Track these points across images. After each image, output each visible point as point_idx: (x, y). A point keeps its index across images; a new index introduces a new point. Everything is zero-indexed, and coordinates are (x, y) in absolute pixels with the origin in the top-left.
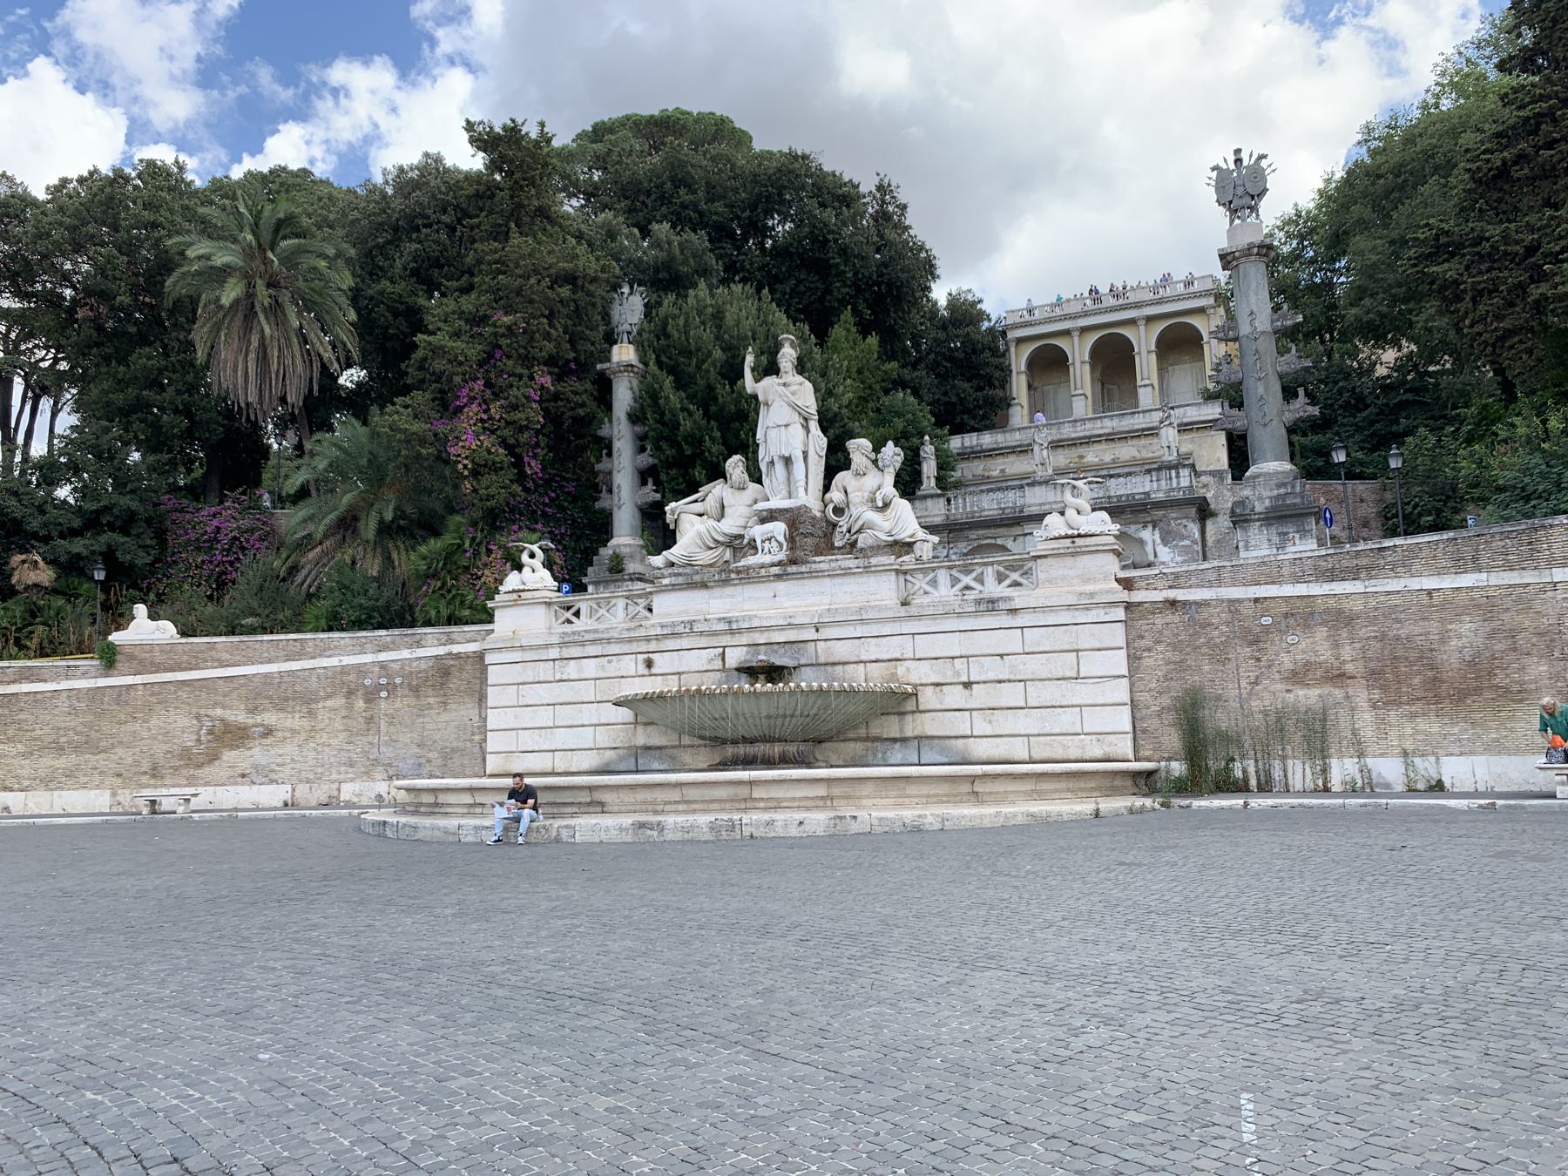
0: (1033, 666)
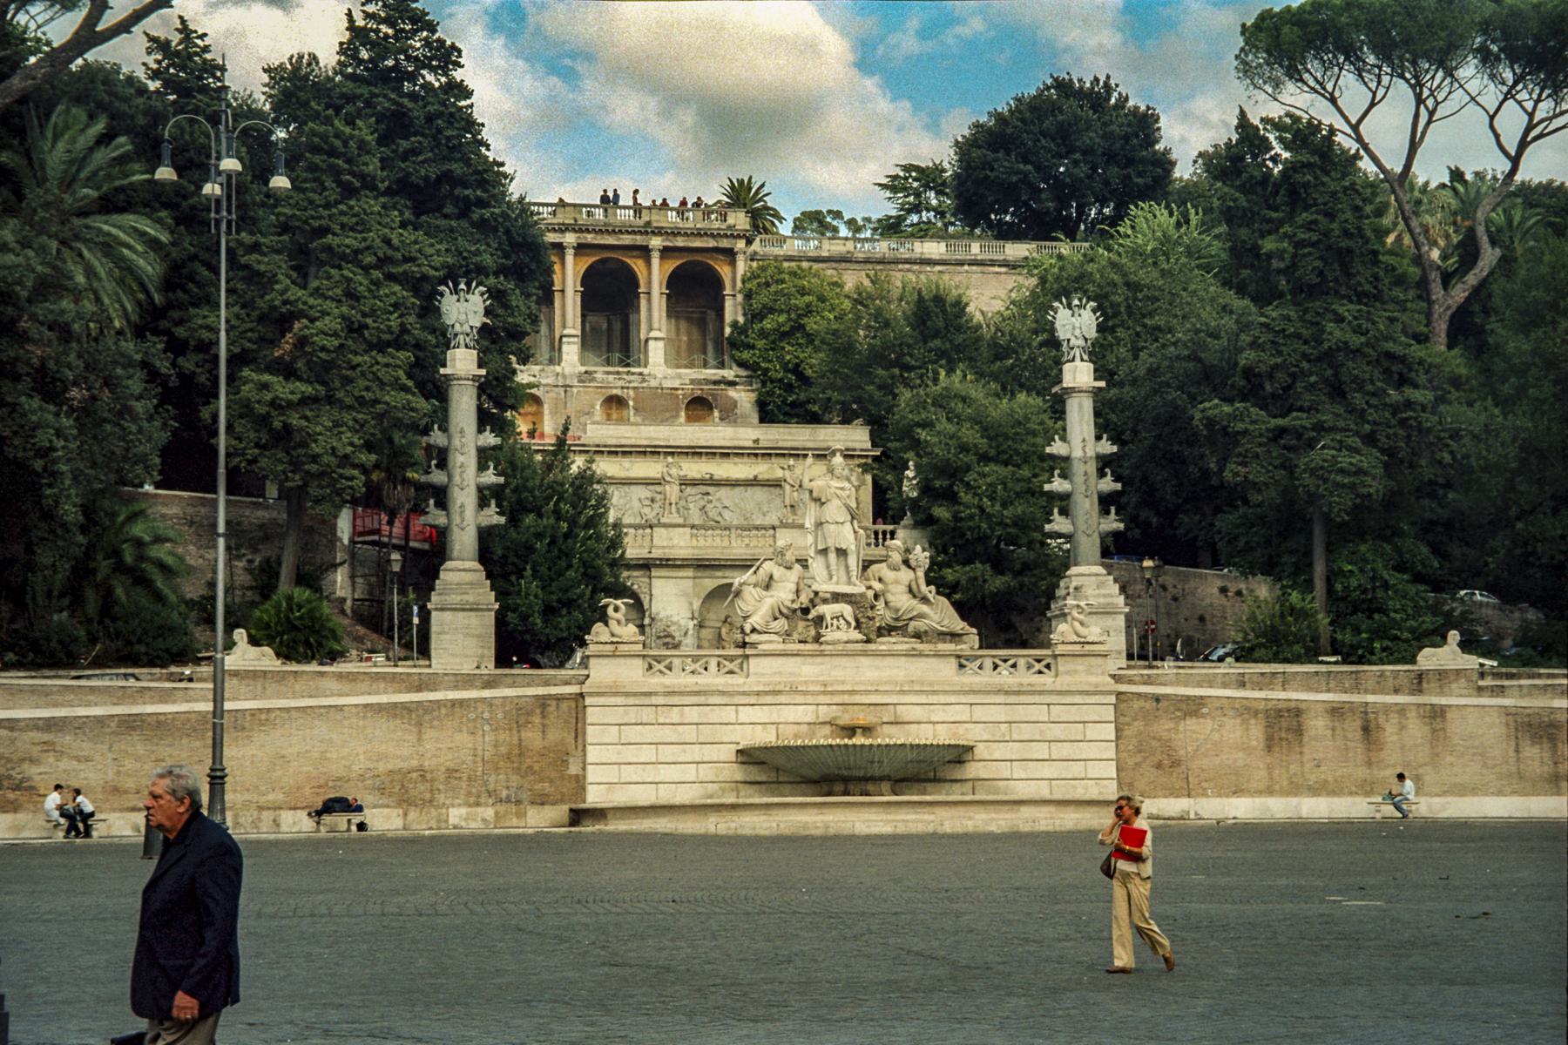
0: (1056, 731)
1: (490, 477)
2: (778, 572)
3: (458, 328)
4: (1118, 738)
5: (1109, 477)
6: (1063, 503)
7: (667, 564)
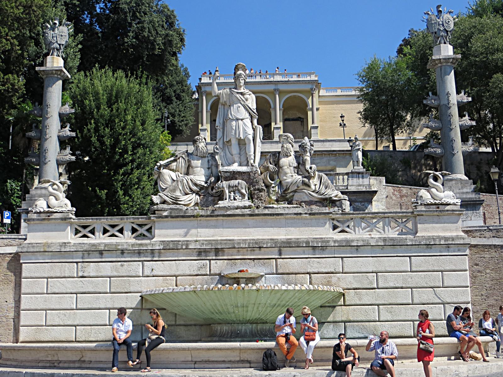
1: (67, 132)
4: (473, 283)
5: (467, 117)
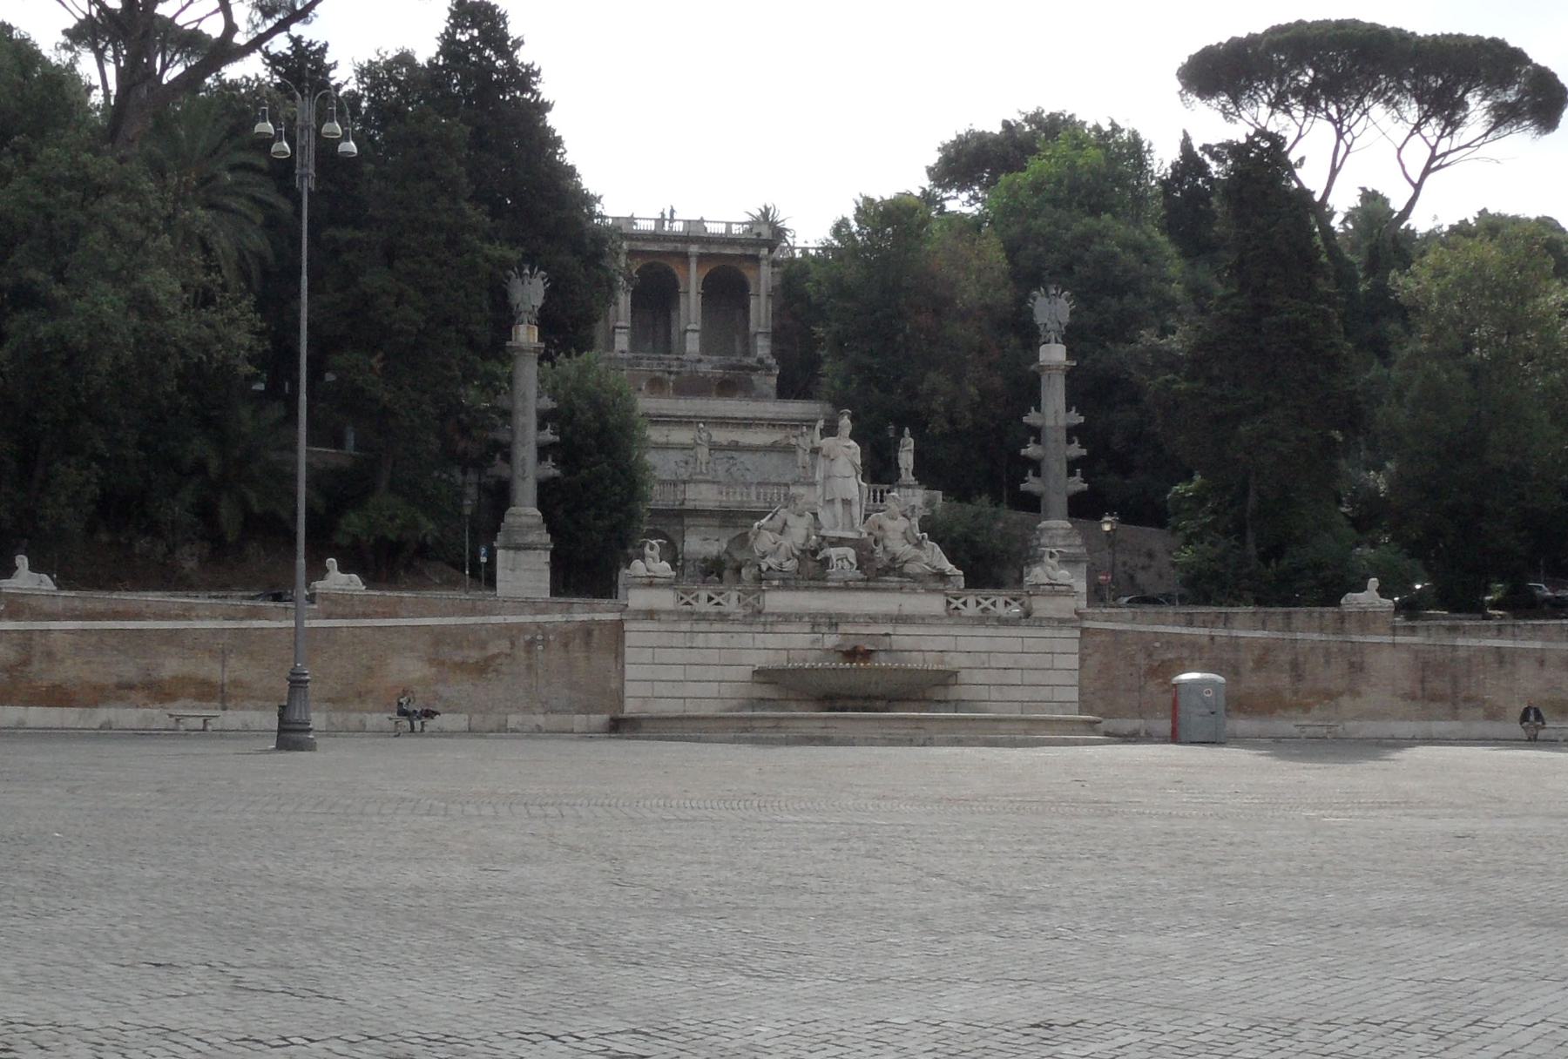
0: (1028, 660)
1: (548, 436)
2: (792, 519)
3: (522, 307)
6: (1036, 466)
7: (696, 513)
